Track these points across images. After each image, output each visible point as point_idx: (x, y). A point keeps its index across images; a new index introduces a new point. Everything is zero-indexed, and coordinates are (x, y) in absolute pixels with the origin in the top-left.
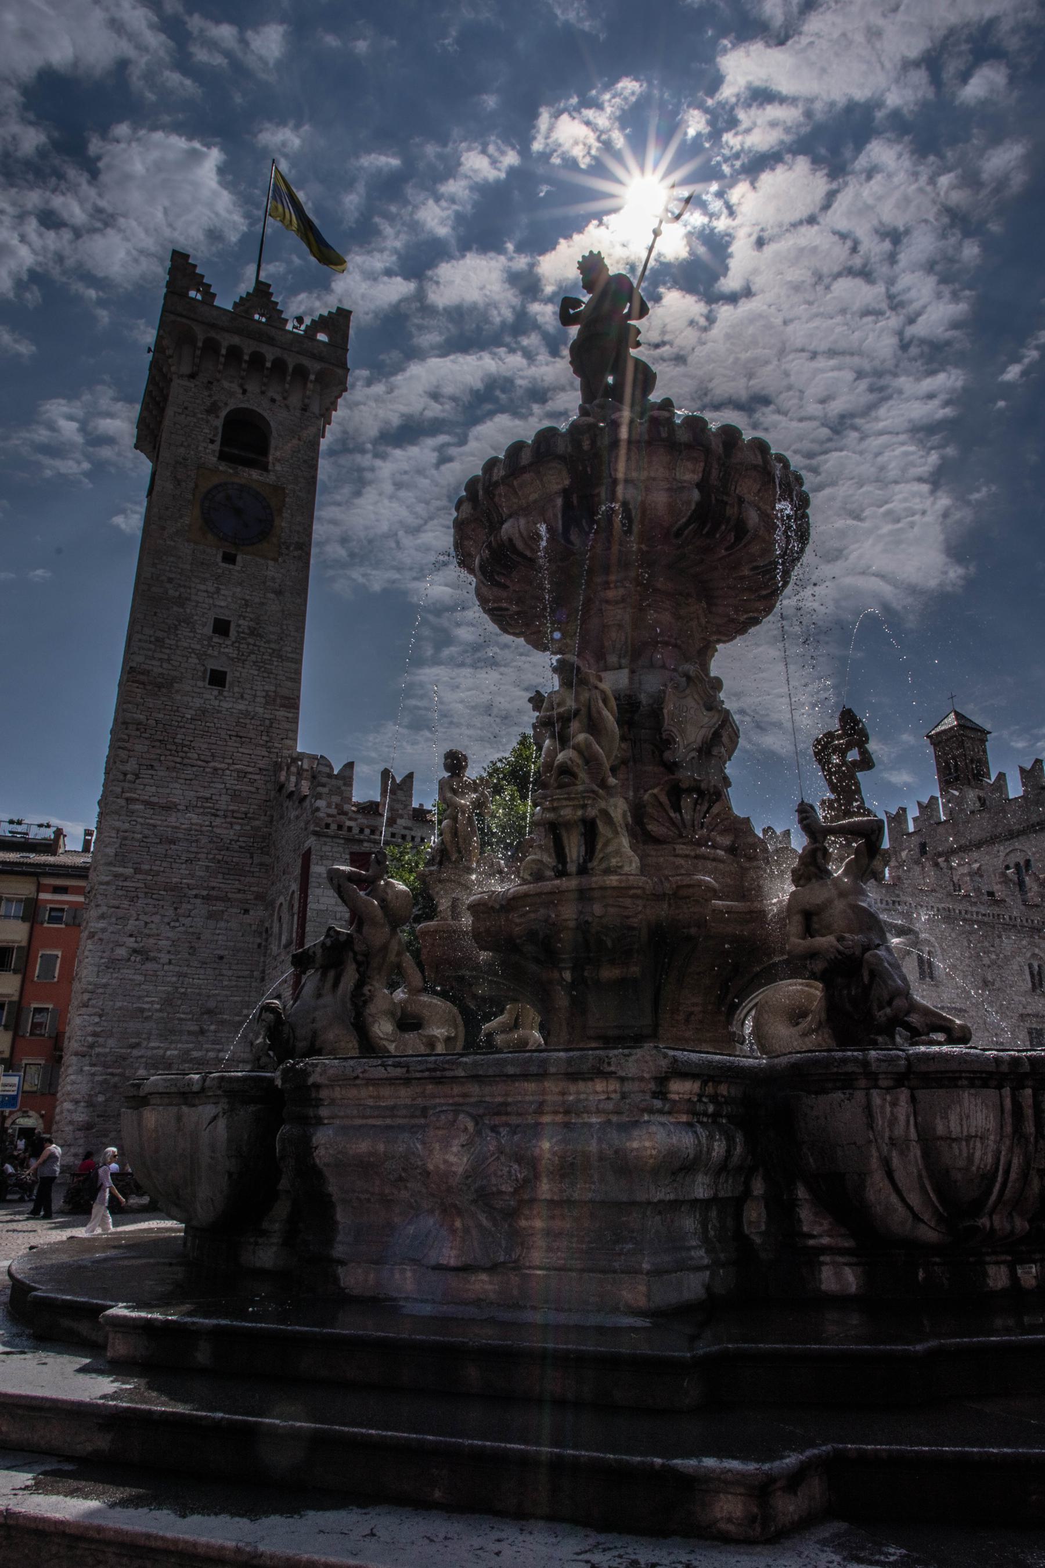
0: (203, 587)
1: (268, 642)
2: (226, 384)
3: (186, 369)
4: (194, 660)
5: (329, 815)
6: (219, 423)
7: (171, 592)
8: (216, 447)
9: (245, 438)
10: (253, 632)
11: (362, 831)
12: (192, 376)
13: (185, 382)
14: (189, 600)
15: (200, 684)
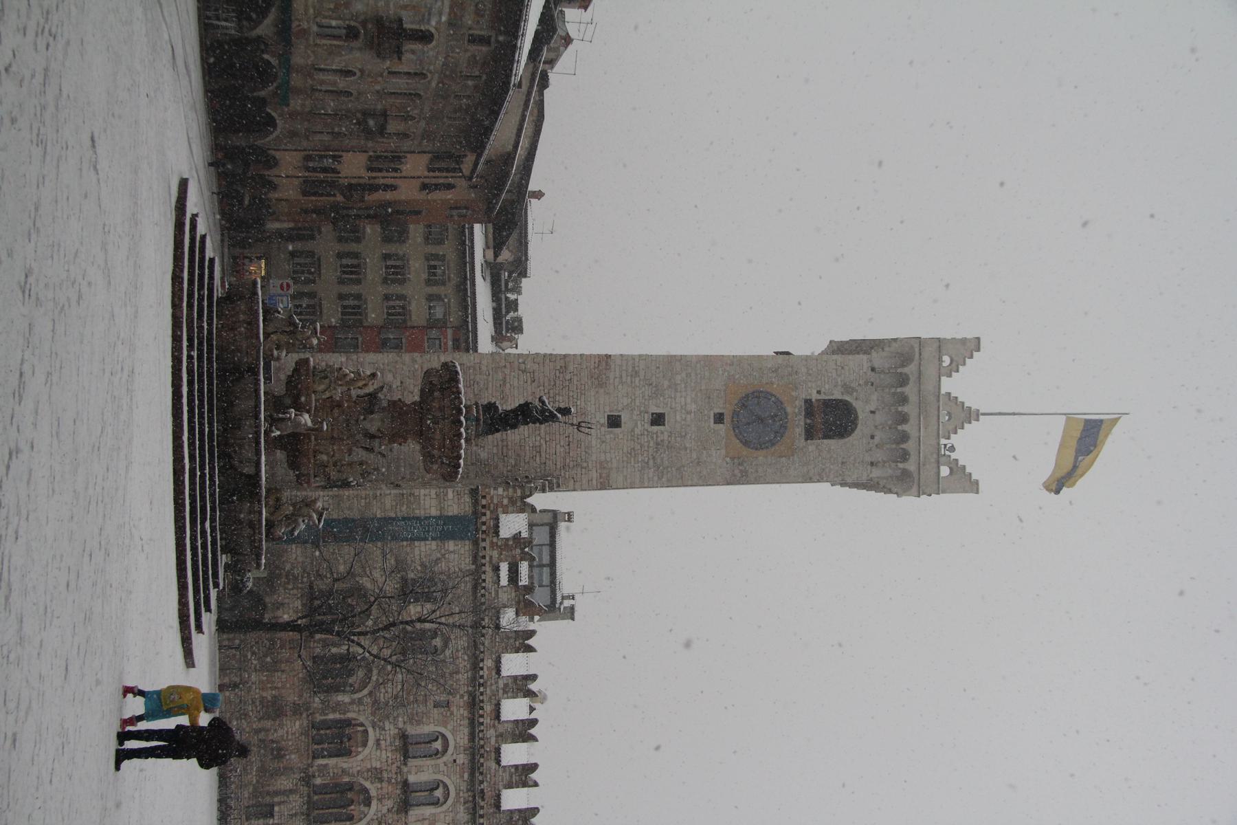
0: (689, 400)
1: (654, 458)
2: (874, 397)
3: (877, 363)
4: (626, 401)
5: (492, 498)
6: (837, 395)
7: (678, 378)
8: (815, 397)
9: (832, 419)
10: (657, 444)
11: (484, 523)
12: (873, 369)
13: (866, 365)
14: (676, 390)
15: (607, 409)
